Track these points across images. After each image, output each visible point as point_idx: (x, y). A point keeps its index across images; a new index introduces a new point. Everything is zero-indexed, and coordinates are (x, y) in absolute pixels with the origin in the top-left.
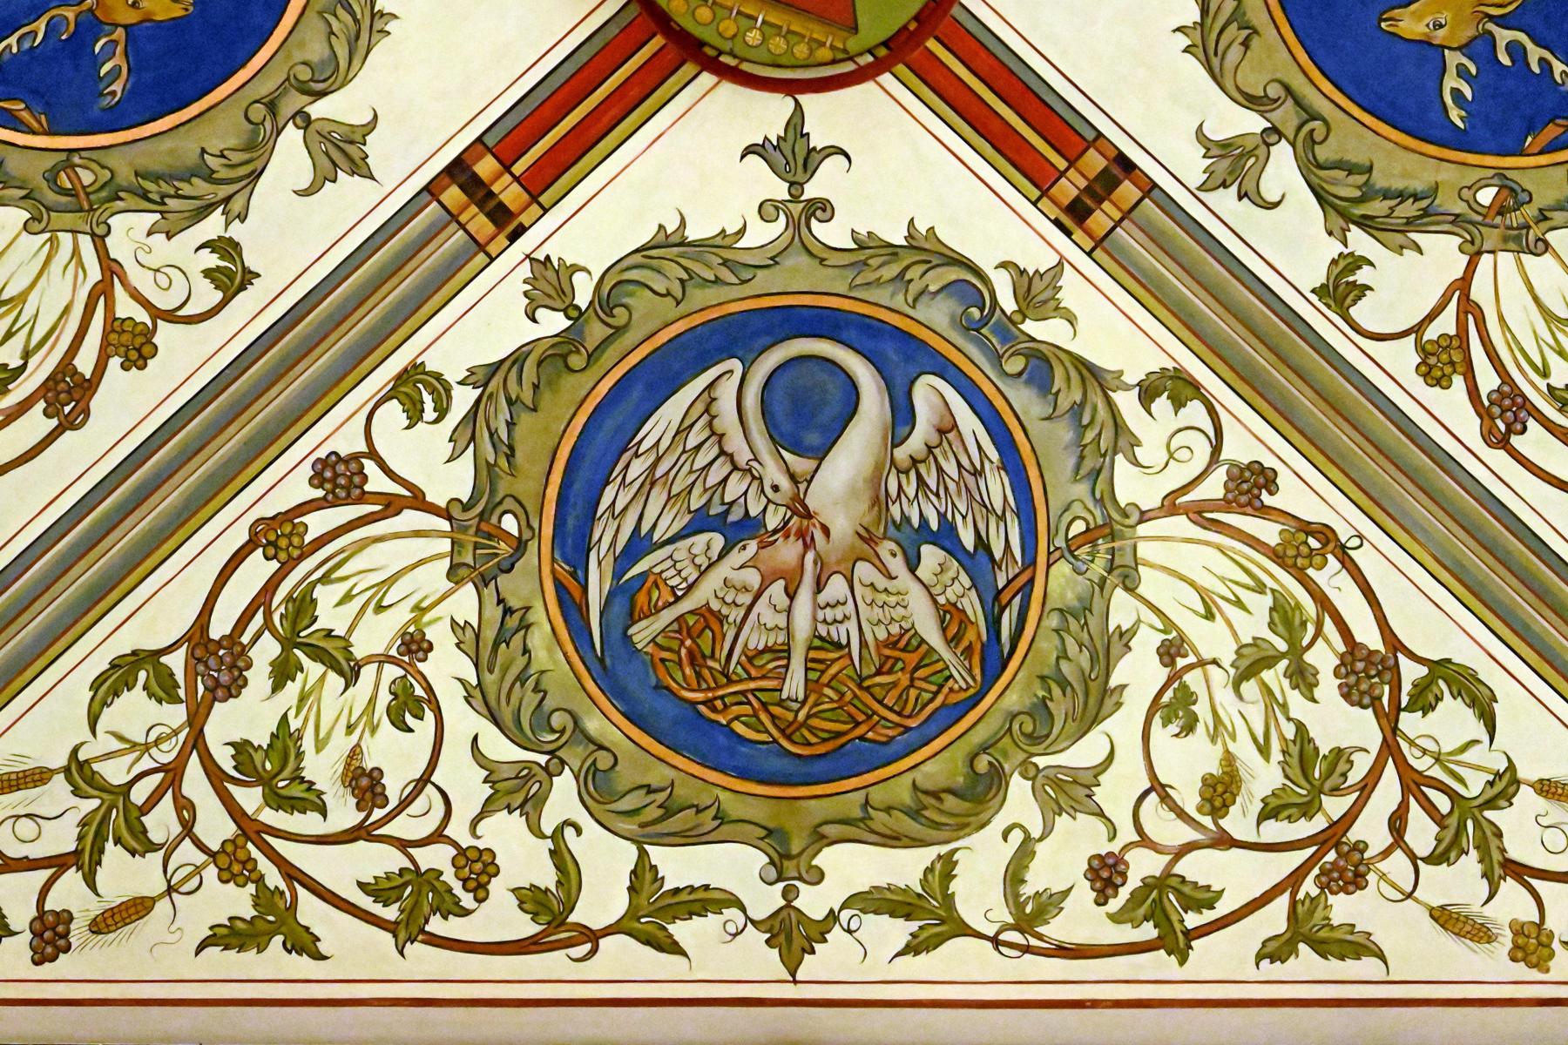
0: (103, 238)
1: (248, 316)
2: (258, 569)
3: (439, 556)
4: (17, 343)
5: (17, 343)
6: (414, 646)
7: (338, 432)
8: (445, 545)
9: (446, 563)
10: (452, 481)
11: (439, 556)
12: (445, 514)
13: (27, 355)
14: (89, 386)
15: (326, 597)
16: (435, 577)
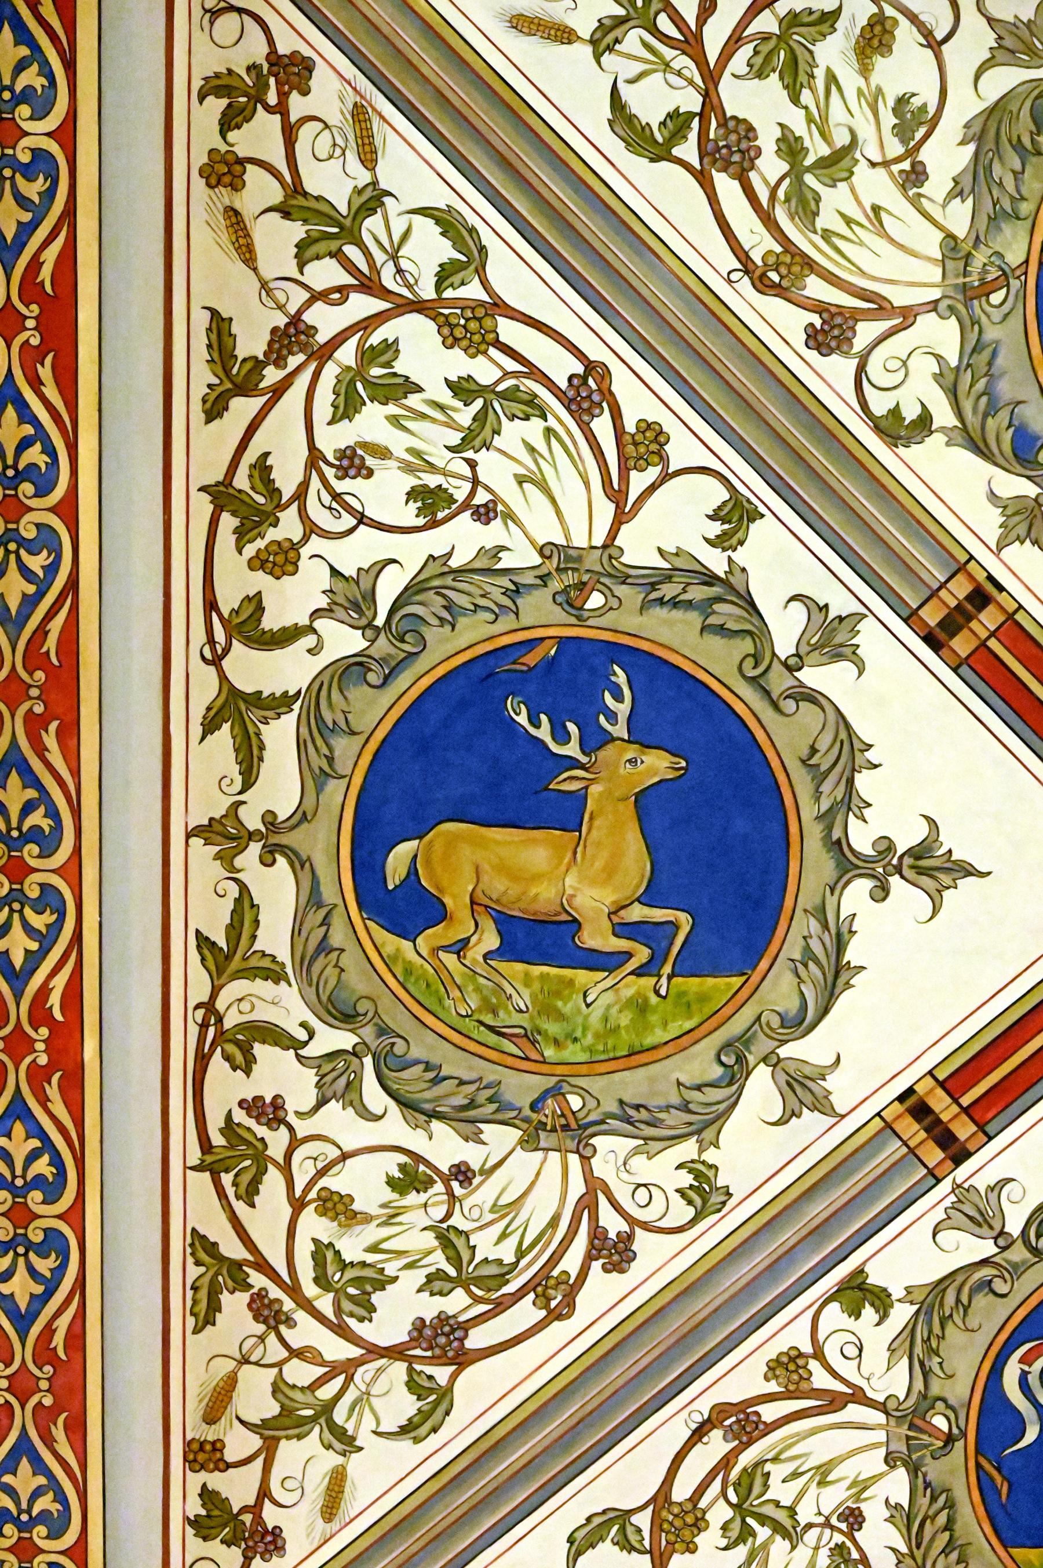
0: (589, 1158)
1: (716, 1230)
2: (716, 1445)
3: (875, 1446)
4: (512, 1242)
5: (512, 1242)
6: (854, 1518)
7: (789, 1332)
8: (881, 1436)
9: (883, 1451)
10: (894, 1382)
11: (875, 1446)
12: (882, 1407)
13: (520, 1254)
14: (573, 1288)
15: (777, 1471)
16: (874, 1462)
